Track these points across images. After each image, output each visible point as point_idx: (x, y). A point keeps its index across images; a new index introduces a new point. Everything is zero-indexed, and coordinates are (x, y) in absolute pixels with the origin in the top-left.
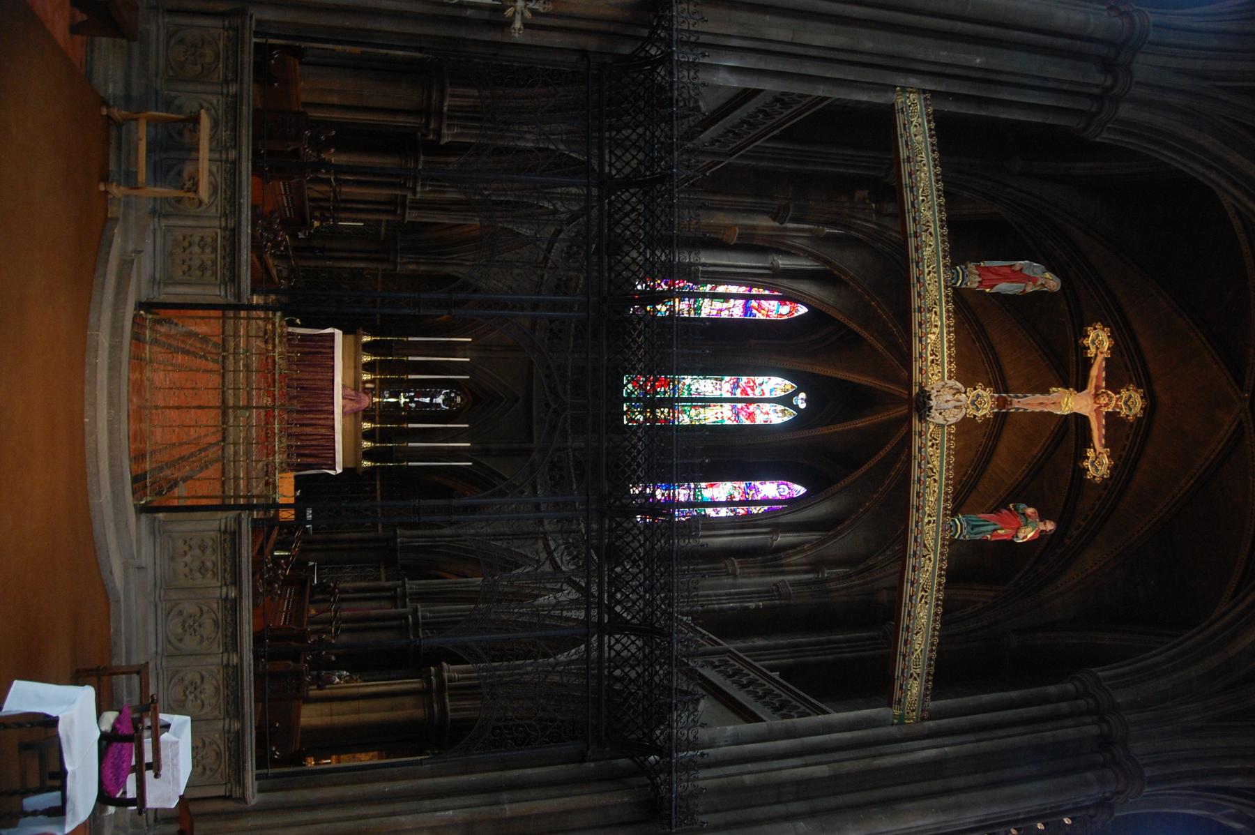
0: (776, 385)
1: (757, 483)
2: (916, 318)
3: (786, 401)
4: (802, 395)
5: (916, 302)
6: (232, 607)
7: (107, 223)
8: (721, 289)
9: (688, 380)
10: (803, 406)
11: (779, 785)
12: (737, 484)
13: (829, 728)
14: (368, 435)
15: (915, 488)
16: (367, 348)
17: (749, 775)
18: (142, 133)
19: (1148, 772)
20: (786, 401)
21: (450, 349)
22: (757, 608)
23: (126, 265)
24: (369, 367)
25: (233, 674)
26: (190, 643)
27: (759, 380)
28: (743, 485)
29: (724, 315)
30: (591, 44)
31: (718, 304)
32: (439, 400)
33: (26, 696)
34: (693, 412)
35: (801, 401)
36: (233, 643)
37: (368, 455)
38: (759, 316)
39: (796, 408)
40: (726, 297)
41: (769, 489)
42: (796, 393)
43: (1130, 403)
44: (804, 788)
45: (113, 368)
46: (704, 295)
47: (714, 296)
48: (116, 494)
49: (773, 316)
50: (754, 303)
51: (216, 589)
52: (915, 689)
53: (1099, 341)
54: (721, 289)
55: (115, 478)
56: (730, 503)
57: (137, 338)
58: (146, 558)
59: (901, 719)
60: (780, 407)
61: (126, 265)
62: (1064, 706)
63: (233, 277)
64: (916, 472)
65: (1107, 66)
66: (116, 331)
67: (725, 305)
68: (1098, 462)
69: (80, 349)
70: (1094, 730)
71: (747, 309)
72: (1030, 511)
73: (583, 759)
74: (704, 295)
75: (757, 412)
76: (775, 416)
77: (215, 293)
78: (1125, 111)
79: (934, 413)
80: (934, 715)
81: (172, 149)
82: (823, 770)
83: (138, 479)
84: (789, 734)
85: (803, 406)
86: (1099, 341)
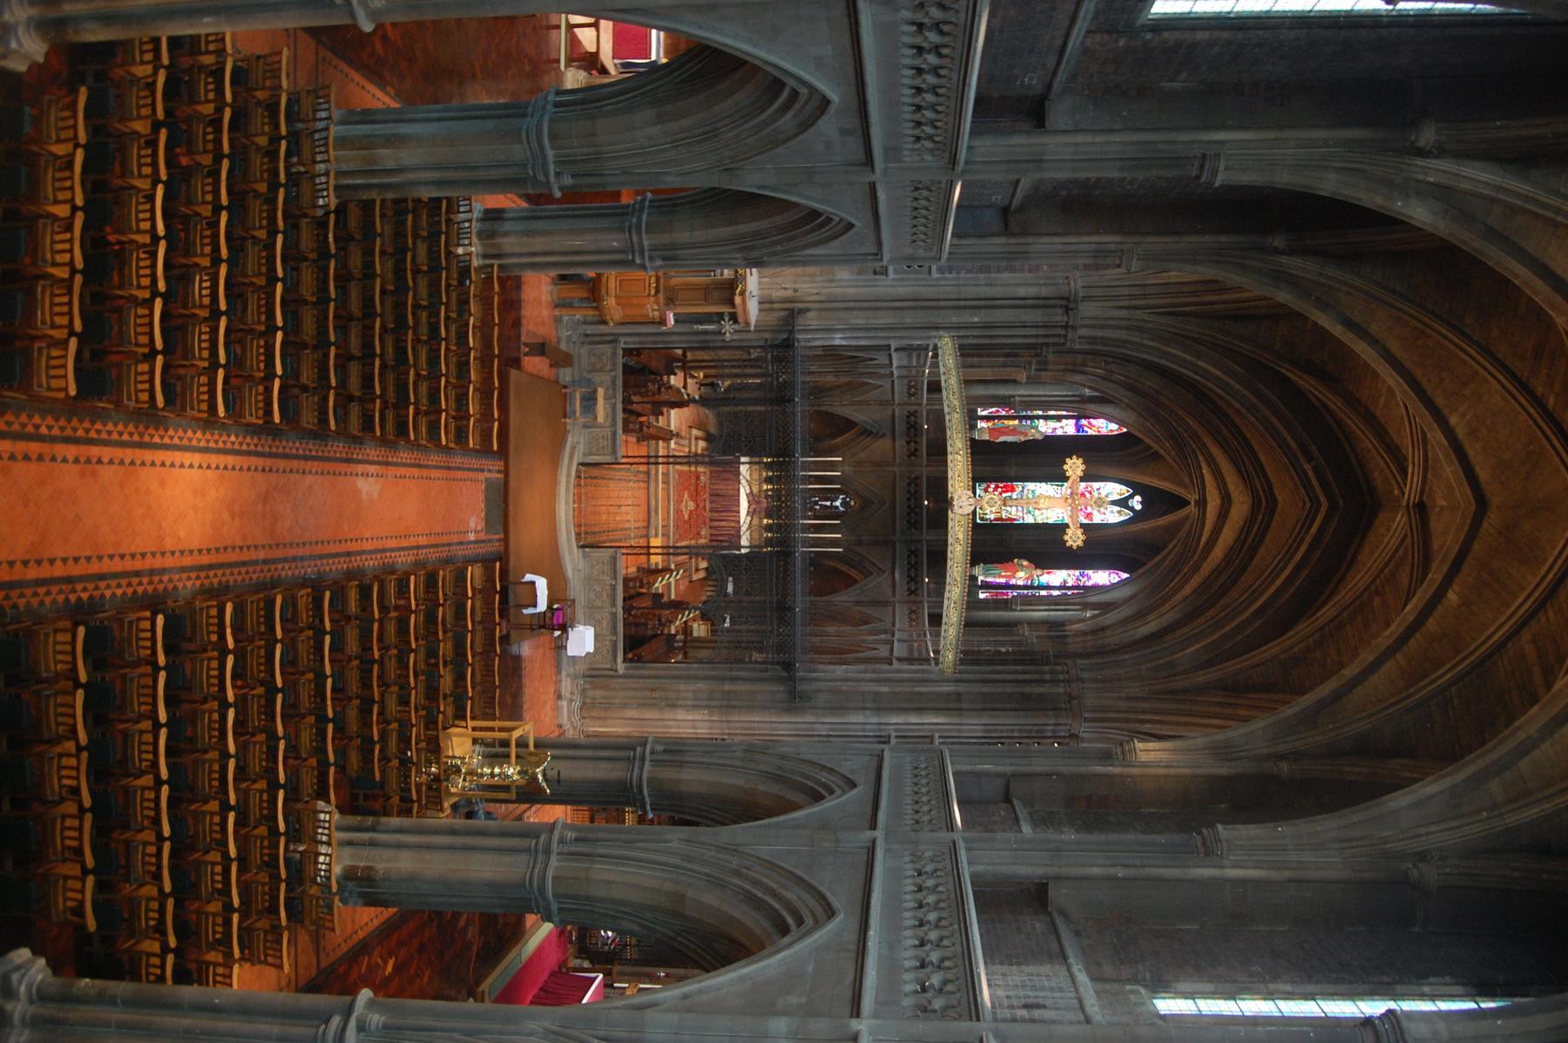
0: (1115, 490)
1: (1090, 572)
2: (950, 457)
3: (1123, 503)
4: (1138, 498)
5: (949, 449)
6: (614, 588)
7: (566, 432)
8: (1052, 413)
9: (1031, 486)
10: (1138, 507)
11: (864, 693)
12: (1071, 572)
14: (768, 528)
16: (768, 466)
17: (845, 687)
18: (578, 396)
19: (1086, 715)
20: (1123, 503)
21: (832, 466)
22: (1007, 653)
23: (573, 448)
24: (768, 480)
25: (614, 615)
26: (598, 603)
27: (1096, 485)
28: (1077, 573)
29: (1059, 432)
30: (767, 335)
31: (1052, 424)
32: (838, 503)
33: (529, 577)
35: (1136, 503)
36: (614, 604)
37: (769, 542)
38: (1091, 432)
39: (1132, 509)
40: (1059, 418)
41: (1101, 577)
42: (1131, 496)
45: (567, 489)
46: (1038, 417)
47: (1046, 418)
48: (569, 540)
49: (1104, 431)
50: (1084, 422)
51: (608, 580)
52: (949, 657)
54: (1052, 413)
55: (568, 532)
56: (1063, 587)
57: (578, 477)
58: (581, 565)
59: (942, 671)
60: (1117, 508)
61: (573, 448)
62: (1048, 677)
63: (614, 452)
64: (950, 540)
65: (1067, 309)
66: (568, 476)
67: (1058, 425)
69: (554, 483)
70: (1061, 690)
71: (1079, 427)
74: (1038, 417)
75: (1095, 513)
76: (1113, 516)
77: (608, 459)
78: (1083, 332)
80: (960, 672)
81: (590, 400)
82: (885, 689)
83: (578, 534)
84: (874, 671)
85: (1138, 507)
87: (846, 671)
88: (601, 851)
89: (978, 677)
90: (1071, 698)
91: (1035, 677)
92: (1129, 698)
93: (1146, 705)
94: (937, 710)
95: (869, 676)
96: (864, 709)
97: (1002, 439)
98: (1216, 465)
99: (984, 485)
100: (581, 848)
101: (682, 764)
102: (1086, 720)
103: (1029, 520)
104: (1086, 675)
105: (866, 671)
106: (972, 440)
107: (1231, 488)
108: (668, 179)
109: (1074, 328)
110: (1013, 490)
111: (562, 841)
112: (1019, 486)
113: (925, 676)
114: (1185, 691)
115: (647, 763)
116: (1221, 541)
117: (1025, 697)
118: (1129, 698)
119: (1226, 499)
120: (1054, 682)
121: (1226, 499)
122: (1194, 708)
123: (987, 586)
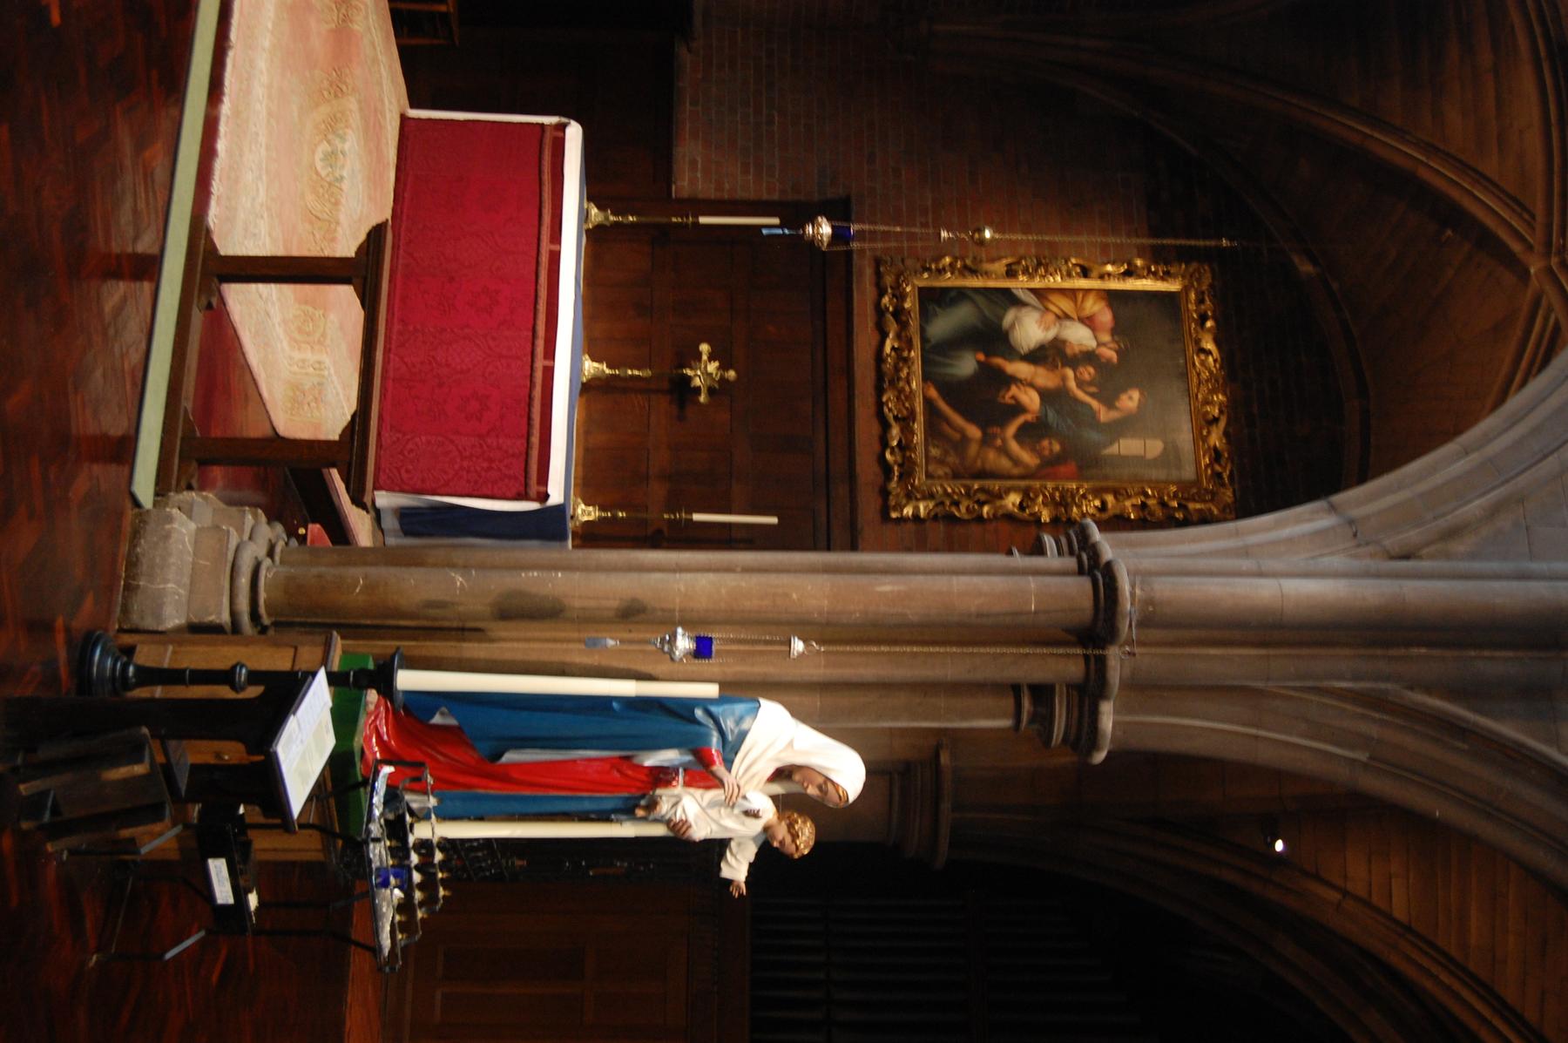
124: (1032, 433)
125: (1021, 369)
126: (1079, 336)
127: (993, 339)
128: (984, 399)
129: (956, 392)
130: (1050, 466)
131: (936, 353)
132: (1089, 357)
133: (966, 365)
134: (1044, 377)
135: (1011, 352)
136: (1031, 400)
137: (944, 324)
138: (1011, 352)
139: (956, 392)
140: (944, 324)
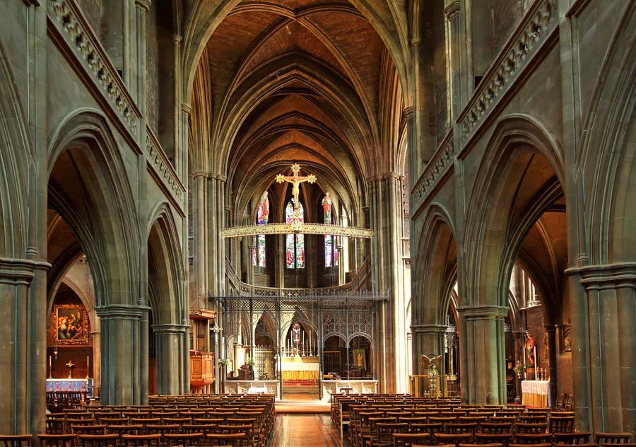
5: (272, 233)
9: (288, 245)
13: (374, 255)
15: (317, 233)
19: (391, 171)
34: (299, 242)
43: (296, 168)
44: (386, 264)
52: (367, 233)
53: (280, 178)
62: (374, 190)
64: (314, 233)
68: (312, 179)
70: (380, 183)
72: (323, 200)
73: (375, 314)
74: (257, 240)
78: (220, 173)
79: (299, 229)
86: (280, 178)
87: (375, 279)
88: (471, 286)
89: (375, 220)
90: (383, 180)
91: (374, 195)
92: (383, 154)
93: (386, 145)
94: (391, 236)
95: (376, 269)
96: (391, 268)
97: (268, 210)
98: (280, 148)
99: (288, 265)
100: (470, 295)
101: (423, 310)
102: (393, 170)
103: (303, 246)
104: (373, 173)
105: (374, 270)
106: (268, 222)
107: (288, 142)
108: (142, 250)
109: (218, 176)
110: (290, 253)
111: (468, 304)
112: (288, 250)
113: (375, 243)
114: (379, 130)
115: (423, 326)
116: (311, 147)
117: (384, 199)
118: (383, 154)
119: (293, 145)
120: (377, 187)
121: (293, 145)
122: (386, 123)
123: (333, 262)
124: (78, 328)
125: (69, 328)
126: (65, 321)
127: (65, 331)
128: (73, 333)
129: (72, 336)
130: (81, 325)
131: (67, 338)
132: (67, 320)
133: (69, 334)
134: (70, 325)
135: (67, 329)
136: (73, 327)
137: (63, 337)
138: (67, 329)
139: (72, 336)
140: (63, 337)
